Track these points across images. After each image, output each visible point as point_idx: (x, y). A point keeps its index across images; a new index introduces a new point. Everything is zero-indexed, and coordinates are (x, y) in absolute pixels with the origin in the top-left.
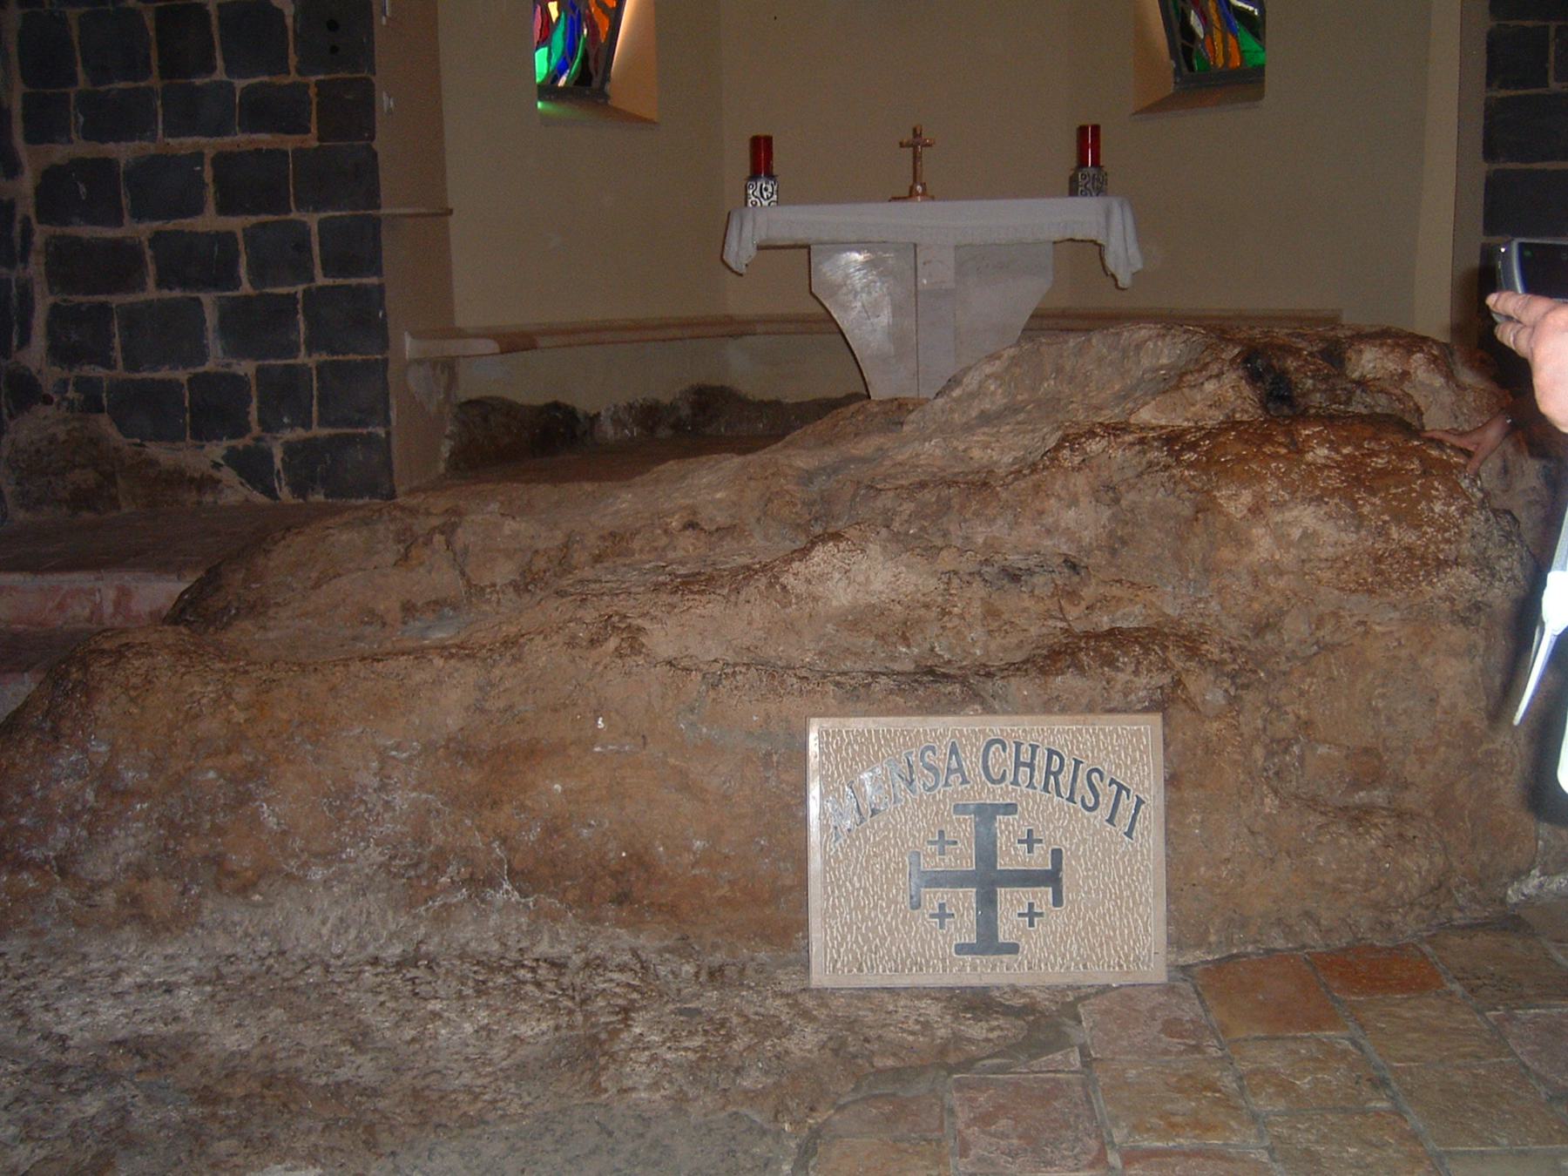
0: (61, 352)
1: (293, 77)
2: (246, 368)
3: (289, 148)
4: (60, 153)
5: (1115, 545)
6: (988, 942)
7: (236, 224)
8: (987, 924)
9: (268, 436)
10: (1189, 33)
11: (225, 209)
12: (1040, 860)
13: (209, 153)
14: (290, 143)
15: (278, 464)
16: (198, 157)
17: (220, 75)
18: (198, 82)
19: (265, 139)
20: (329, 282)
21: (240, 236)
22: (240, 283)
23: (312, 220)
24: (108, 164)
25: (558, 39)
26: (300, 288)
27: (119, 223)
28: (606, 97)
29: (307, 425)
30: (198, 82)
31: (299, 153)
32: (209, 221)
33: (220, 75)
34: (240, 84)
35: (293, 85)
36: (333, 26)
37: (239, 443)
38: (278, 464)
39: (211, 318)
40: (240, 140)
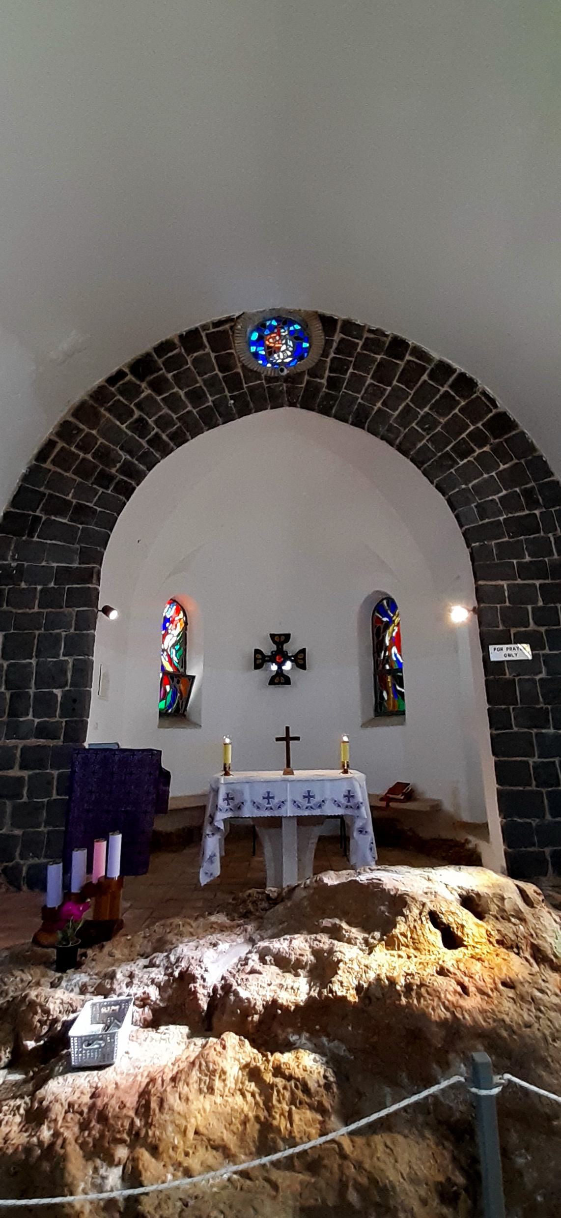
1: (57, 719)
2: (18, 832)
3: (52, 745)
7: (25, 774)
9: (22, 862)
11: (22, 768)
13: (20, 746)
14: (52, 743)
15: (24, 874)
16: (16, 747)
17: (30, 717)
18: (21, 719)
19: (42, 742)
20: (59, 797)
21: (26, 778)
22: (23, 796)
23: (55, 773)
25: (169, 698)
26: (46, 800)
28: (185, 716)
29: (39, 858)
30: (21, 719)
31: (56, 747)
33: (30, 717)
34: (37, 720)
35: (57, 722)
36: (75, 701)
37: (10, 864)
38: (24, 874)
39: (9, 810)
40: (33, 742)
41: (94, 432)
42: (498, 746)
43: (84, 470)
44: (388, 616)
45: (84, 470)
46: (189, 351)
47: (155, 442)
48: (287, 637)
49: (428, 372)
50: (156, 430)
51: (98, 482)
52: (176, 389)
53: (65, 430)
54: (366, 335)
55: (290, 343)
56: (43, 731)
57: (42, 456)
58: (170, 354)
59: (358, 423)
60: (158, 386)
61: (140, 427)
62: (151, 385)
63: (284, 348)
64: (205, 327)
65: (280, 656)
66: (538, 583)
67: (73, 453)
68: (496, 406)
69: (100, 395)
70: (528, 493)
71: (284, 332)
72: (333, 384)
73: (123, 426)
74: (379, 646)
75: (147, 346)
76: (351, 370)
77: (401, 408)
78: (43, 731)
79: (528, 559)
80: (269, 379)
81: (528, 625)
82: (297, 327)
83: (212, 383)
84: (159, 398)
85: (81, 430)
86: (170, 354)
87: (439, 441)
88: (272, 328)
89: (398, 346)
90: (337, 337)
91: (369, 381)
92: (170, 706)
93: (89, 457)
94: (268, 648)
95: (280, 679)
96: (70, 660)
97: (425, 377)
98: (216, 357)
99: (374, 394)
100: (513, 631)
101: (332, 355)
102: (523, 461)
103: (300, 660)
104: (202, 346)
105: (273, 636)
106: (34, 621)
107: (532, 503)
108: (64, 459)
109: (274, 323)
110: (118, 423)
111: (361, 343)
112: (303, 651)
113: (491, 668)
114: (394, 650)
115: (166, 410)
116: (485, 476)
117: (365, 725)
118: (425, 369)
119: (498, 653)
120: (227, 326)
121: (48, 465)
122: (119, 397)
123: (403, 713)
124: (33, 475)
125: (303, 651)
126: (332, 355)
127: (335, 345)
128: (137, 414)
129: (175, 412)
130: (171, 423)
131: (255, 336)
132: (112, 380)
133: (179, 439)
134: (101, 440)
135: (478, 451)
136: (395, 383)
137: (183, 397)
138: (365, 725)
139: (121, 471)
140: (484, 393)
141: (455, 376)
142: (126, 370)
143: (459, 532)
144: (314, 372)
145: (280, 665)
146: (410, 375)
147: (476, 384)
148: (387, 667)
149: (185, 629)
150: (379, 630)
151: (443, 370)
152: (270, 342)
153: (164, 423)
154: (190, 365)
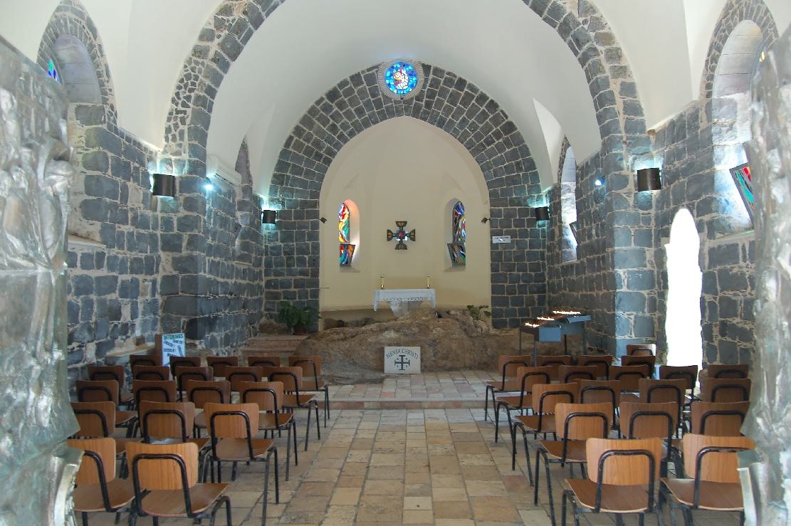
0: (266, 310)
4: (269, 278)
5: (419, 332)
6: (402, 369)
7: (296, 290)
8: (402, 359)
10: (454, 256)
11: (295, 287)
12: (408, 361)
14: (305, 278)
19: (302, 277)
23: (309, 289)
24: (277, 280)
25: (343, 257)
26: (306, 300)
27: (278, 289)
32: (292, 289)
40: (299, 277)
41: (311, 132)
42: (495, 278)
43: (308, 152)
44: (461, 212)
45: (308, 152)
46: (356, 85)
47: (341, 136)
48: (405, 223)
49: (475, 98)
50: (341, 130)
51: (315, 158)
52: (350, 107)
53: (298, 131)
54: (446, 76)
55: (407, 78)
56: (302, 273)
57: (288, 144)
58: (346, 87)
59: (441, 124)
60: (341, 105)
61: (333, 129)
62: (337, 105)
63: (403, 80)
64: (363, 72)
65: (401, 234)
66: (517, 208)
67: (302, 143)
68: (507, 118)
69: (312, 111)
70: (518, 164)
71: (404, 72)
72: (428, 105)
73: (325, 129)
74: (456, 228)
75: (334, 84)
76: (437, 97)
77: (461, 118)
78: (302, 273)
79: (514, 196)
80: (396, 102)
81: (511, 227)
82: (410, 68)
83: (368, 104)
84: (341, 113)
85: (304, 131)
86: (346, 87)
87: (478, 137)
88: (397, 69)
89: (462, 83)
90: (431, 76)
91: (446, 103)
92: (343, 261)
93: (310, 145)
94: (395, 229)
95: (401, 246)
96: (310, 243)
97: (473, 101)
98: (369, 89)
99: (448, 110)
100: (504, 230)
101: (428, 87)
102: (517, 147)
103: (412, 236)
104: (362, 83)
105: (397, 222)
106: (293, 226)
107: (520, 169)
108: (298, 146)
109: (399, 66)
110: (322, 126)
111: (442, 80)
112: (414, 231)
113: (494, 246)
114: (463, 231)
115: (345, 119)
116: (499, 155)
117: (446, 271)
118: (473, 97)
119: (496, 240)
120: (374, 71)
121: (290, 149)
122: (322, 112)
123: (464, 264)
124: (284, 153)
125: (414, 231)
126: (428, 87)
127: (429, 82)
128: (331, 121)
129: (350, 120)
130: (349, 127)
131: (388, 74)
132: (318, 102)
133: (352, 134)
134: (315, 136)
135: (497, 142)
136: (458, 104)
137: (354, 112)
138: (446, 271)
139: (325, 152)
140: (502, 111)
141: (488, 101)
142: (324, 97)
143: (485, 182)
144: (419, 98)
145: (402, 238)
146: (468, 97)
147: (498, 106)
148: (459, 239)
149: (349, 218)
150: (456, 221)
151: (483, 98)
152: (398, 76)
153: (345, 126)
154: (356, 93)
